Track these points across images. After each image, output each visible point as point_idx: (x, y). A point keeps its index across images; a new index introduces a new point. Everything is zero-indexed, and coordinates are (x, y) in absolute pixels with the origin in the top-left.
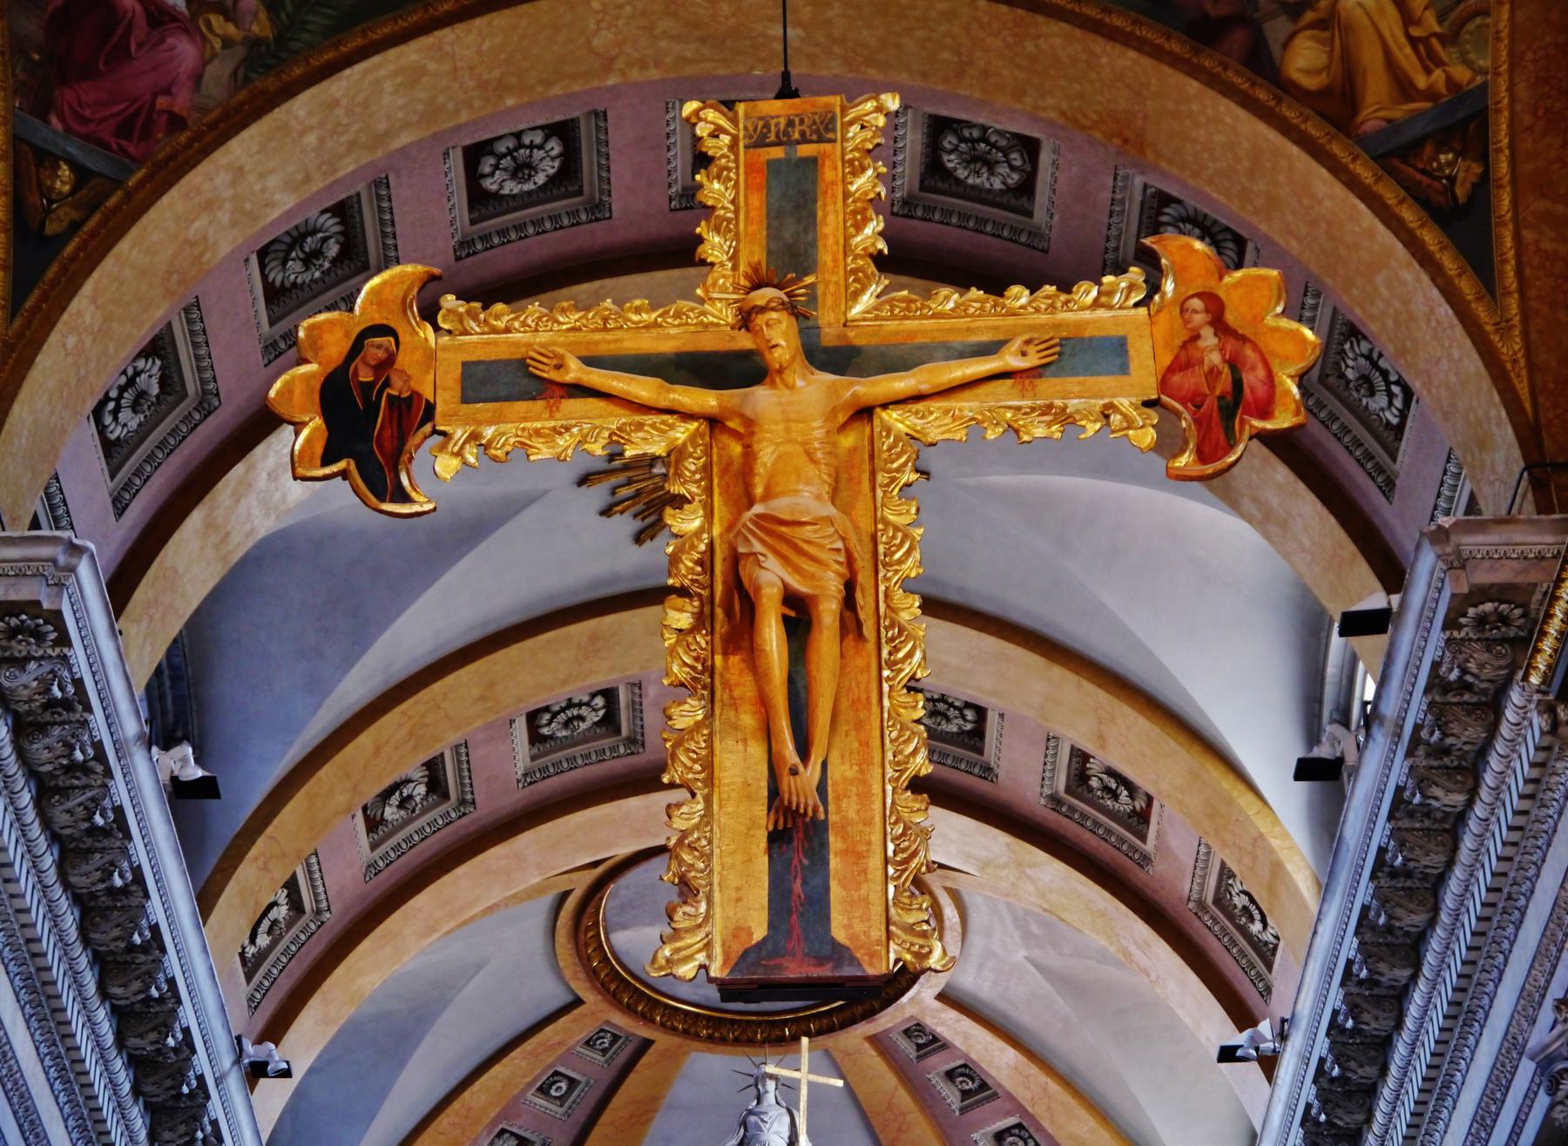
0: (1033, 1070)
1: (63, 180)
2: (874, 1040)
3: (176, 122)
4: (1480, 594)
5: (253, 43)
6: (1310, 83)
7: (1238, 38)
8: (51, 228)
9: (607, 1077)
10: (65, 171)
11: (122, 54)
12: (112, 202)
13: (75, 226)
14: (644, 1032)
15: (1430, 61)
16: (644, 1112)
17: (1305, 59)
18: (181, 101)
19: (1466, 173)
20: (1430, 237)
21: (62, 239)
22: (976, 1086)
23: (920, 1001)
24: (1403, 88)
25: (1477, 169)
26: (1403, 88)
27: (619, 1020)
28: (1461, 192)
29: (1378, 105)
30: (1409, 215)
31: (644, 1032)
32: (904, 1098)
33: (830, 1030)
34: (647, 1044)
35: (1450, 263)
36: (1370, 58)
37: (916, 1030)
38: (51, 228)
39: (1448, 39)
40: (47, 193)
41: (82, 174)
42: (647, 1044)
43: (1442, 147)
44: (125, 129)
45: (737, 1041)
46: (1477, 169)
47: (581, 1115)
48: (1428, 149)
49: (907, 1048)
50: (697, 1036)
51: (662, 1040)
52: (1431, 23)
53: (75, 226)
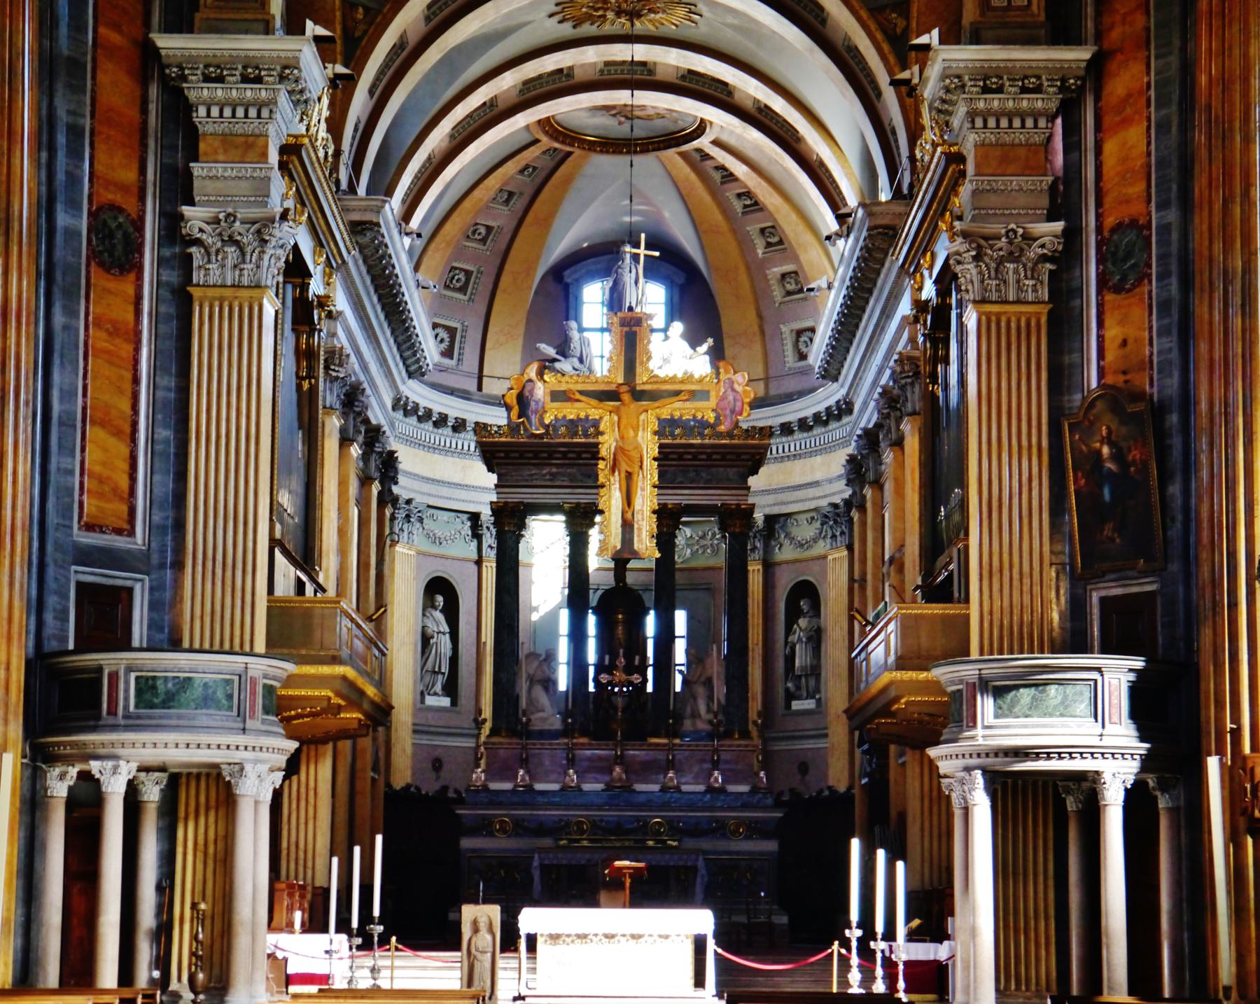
0: (754, 175)
1: (360, 13)
2: (681, 154)
4: (876, 227)
8: (357, 34)
9: (552, 164)
10: (361, 10)
12: (378, 20)
13: (365, 32)
14: (568, 149)
16: (569, 180)
19: (901, 24)
20: (886, 47)
21: (361, 38)
22: (729, 177)
23: (703, 142)
25: (905, 23)
27: (557, 145)
28: (899, 31)
30: (879, 36)
31: (568, 149)
32: (693, 176)
33: (659, 149)
34: (569, 154)
35: (892, 59)
38: (357, 34)
40: (354, 20)
41: (367, 10)
42: (569, 154)
43: (893, 12)
45: (614, 152)
46: (905, 23)
47: (538, 180)
48: (888, 11)
49: (697, 156)
50: (595, 151)
51: (578, 152)
53: (365, 32)
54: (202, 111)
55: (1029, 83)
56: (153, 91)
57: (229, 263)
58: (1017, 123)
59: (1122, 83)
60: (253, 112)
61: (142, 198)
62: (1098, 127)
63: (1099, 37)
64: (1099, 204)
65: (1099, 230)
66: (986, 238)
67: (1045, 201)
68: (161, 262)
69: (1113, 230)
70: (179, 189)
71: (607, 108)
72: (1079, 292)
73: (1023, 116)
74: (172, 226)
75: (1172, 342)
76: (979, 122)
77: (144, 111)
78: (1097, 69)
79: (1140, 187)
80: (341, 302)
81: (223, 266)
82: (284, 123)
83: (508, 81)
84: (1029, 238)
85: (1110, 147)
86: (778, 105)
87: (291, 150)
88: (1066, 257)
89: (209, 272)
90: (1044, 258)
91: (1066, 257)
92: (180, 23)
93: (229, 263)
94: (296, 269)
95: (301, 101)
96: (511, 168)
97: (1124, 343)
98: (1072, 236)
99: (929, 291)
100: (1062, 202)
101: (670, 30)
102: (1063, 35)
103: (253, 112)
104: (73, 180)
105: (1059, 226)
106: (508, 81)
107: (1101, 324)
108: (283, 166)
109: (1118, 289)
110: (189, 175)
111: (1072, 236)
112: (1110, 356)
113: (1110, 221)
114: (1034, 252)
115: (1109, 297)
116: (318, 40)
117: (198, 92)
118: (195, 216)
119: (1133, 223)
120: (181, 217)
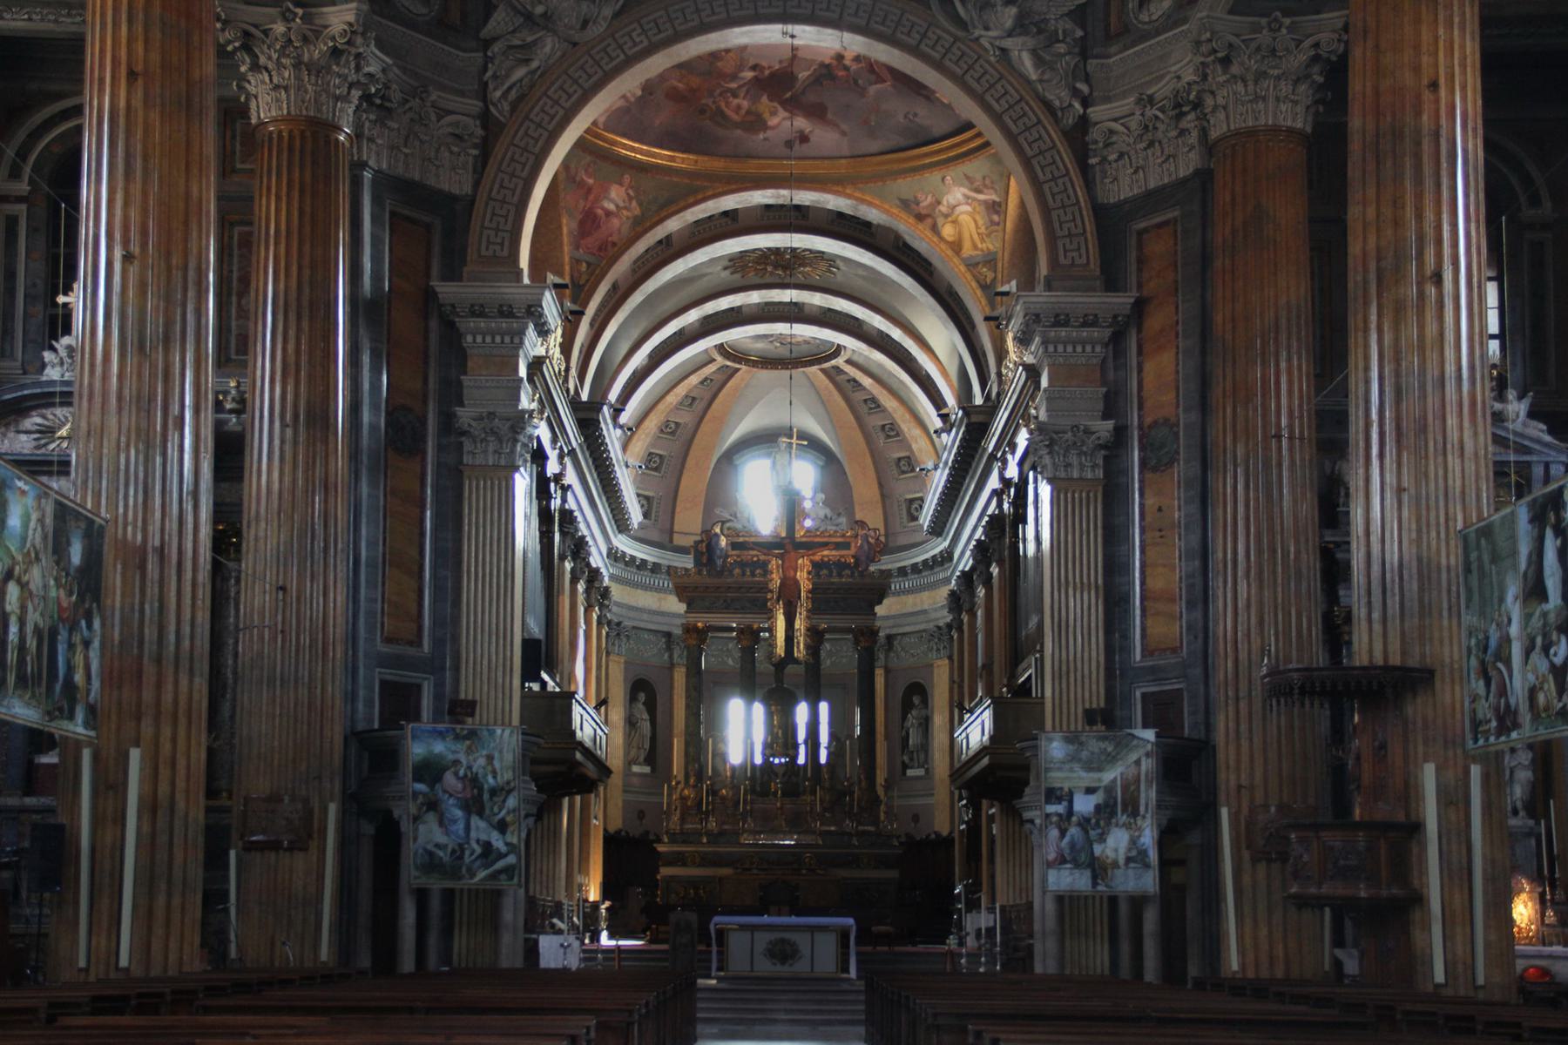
3: (614, 244)
5: (636, 217)
6: (950, 239)
7: (929, 221)
11: (599, 227)
15: (983, 241)
17: (948, 231)
18: (615, 238)
19: (990, 275)
24: (975, 247)
26: (975, 247)
29: (967, 251)
36: (966, 236)
37: (837, 368)
39: (989, 235)
41: (589, 264)
44: (600, 249)
52: (983, 230)
54: (469, 338)
55: (1090, 322)
56: (434, 324)
57: (491, 449)
58: (1079, 349)
59: (1156, 320)
60: (507, 339)
61: (425, 402)
62: (1140, 352)
63: (1140, 286)
64: (1140, 408)
65: (1140, 427)
66: (1057, 433)
67: (1101, 406)
68: (440, 448)
69: (1150, 427)
70: (452, 394)
71: (765, 336)
72: (1127, 472)
73: (1084, 343)
74: (448, 423)
75: (1195, 509)
76: (1051, 348)
77: (426, 338)
78: (1140, 306)
79: (1172, 395)
80: (571, 478)
81: (485, 452)
82: (533, 346)
83: (693, 316)
84: (1088, 432)
85: (1149, 367)
86: (896, 334)
87: (536, 365)
88: (1116, 445)
89: (475, 455)
90: (1101, 447)
91: (1116, 445)
92: (452, 273)
93: (491, 449)
94: (539, 456)
95: (543, 332)
96: (694, 380)
97: (1160, 509)
98: (1121, 433)
99: (1012, 472)
100: (1112, 406)
101: (816, 278)
102: (1112, 282)
103: (507, 339)
104: (376, 386)
105: (1110, 424)
106: (693, 316)
107: (1142, 495)
108: (530, 380)
109: (1155, 469)
110: (460, 383)
111: (1121, 433)
112: (1148, 519)
113: (1148, 420)
114: (1091, 441)
115: (1149, 475)
116: (556, 286)
117: (467, 324)
118: (465, 415)
119: (1166, 420)
120: (454, 415)
